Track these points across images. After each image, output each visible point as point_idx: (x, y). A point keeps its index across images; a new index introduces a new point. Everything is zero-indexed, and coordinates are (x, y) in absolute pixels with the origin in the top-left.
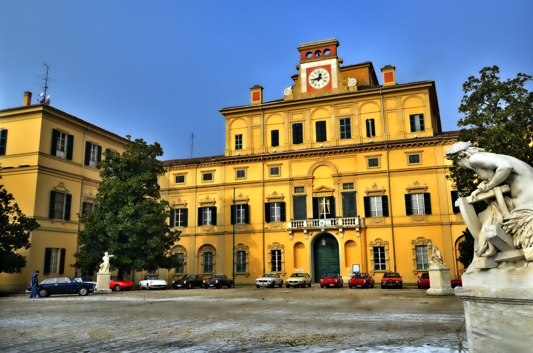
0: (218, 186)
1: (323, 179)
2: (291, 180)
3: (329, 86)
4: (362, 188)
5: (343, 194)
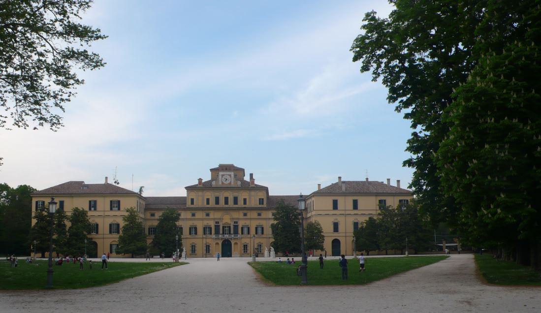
0: (183, 219)
1: (227, 219)
2: (214, 219)
4: (241, 224)
5: (234, 225)
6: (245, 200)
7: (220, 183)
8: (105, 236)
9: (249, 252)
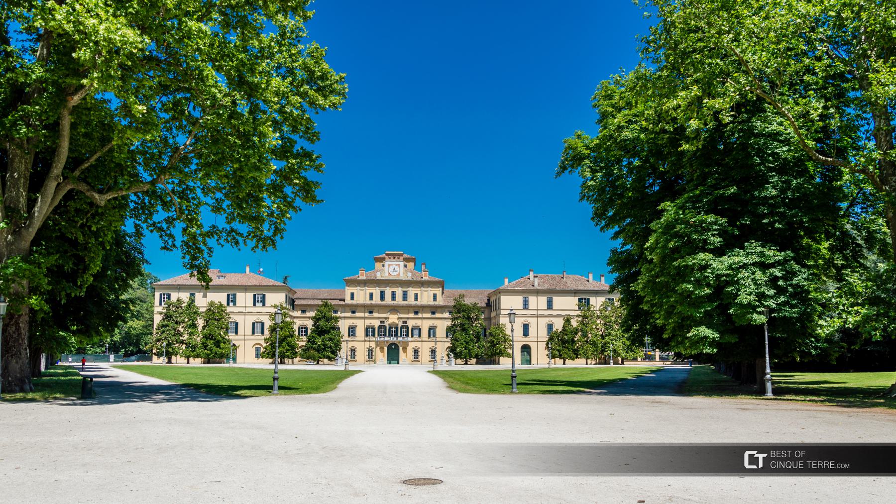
1: (393, 319)
2: (379, 318)
3: (399, 274)
4: (411, 324)
6: (416, 295)
7: (387, 274)
8: (246, 337)
9: (420, 358)
